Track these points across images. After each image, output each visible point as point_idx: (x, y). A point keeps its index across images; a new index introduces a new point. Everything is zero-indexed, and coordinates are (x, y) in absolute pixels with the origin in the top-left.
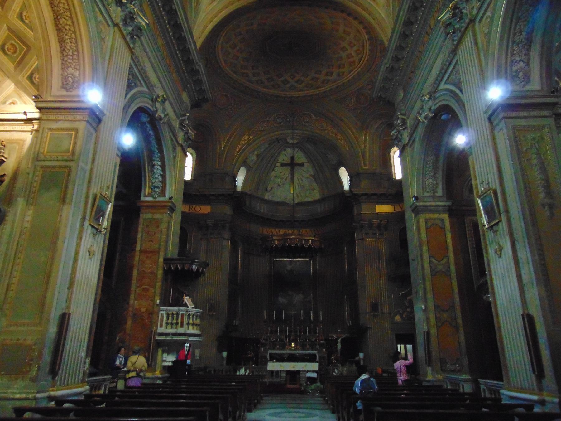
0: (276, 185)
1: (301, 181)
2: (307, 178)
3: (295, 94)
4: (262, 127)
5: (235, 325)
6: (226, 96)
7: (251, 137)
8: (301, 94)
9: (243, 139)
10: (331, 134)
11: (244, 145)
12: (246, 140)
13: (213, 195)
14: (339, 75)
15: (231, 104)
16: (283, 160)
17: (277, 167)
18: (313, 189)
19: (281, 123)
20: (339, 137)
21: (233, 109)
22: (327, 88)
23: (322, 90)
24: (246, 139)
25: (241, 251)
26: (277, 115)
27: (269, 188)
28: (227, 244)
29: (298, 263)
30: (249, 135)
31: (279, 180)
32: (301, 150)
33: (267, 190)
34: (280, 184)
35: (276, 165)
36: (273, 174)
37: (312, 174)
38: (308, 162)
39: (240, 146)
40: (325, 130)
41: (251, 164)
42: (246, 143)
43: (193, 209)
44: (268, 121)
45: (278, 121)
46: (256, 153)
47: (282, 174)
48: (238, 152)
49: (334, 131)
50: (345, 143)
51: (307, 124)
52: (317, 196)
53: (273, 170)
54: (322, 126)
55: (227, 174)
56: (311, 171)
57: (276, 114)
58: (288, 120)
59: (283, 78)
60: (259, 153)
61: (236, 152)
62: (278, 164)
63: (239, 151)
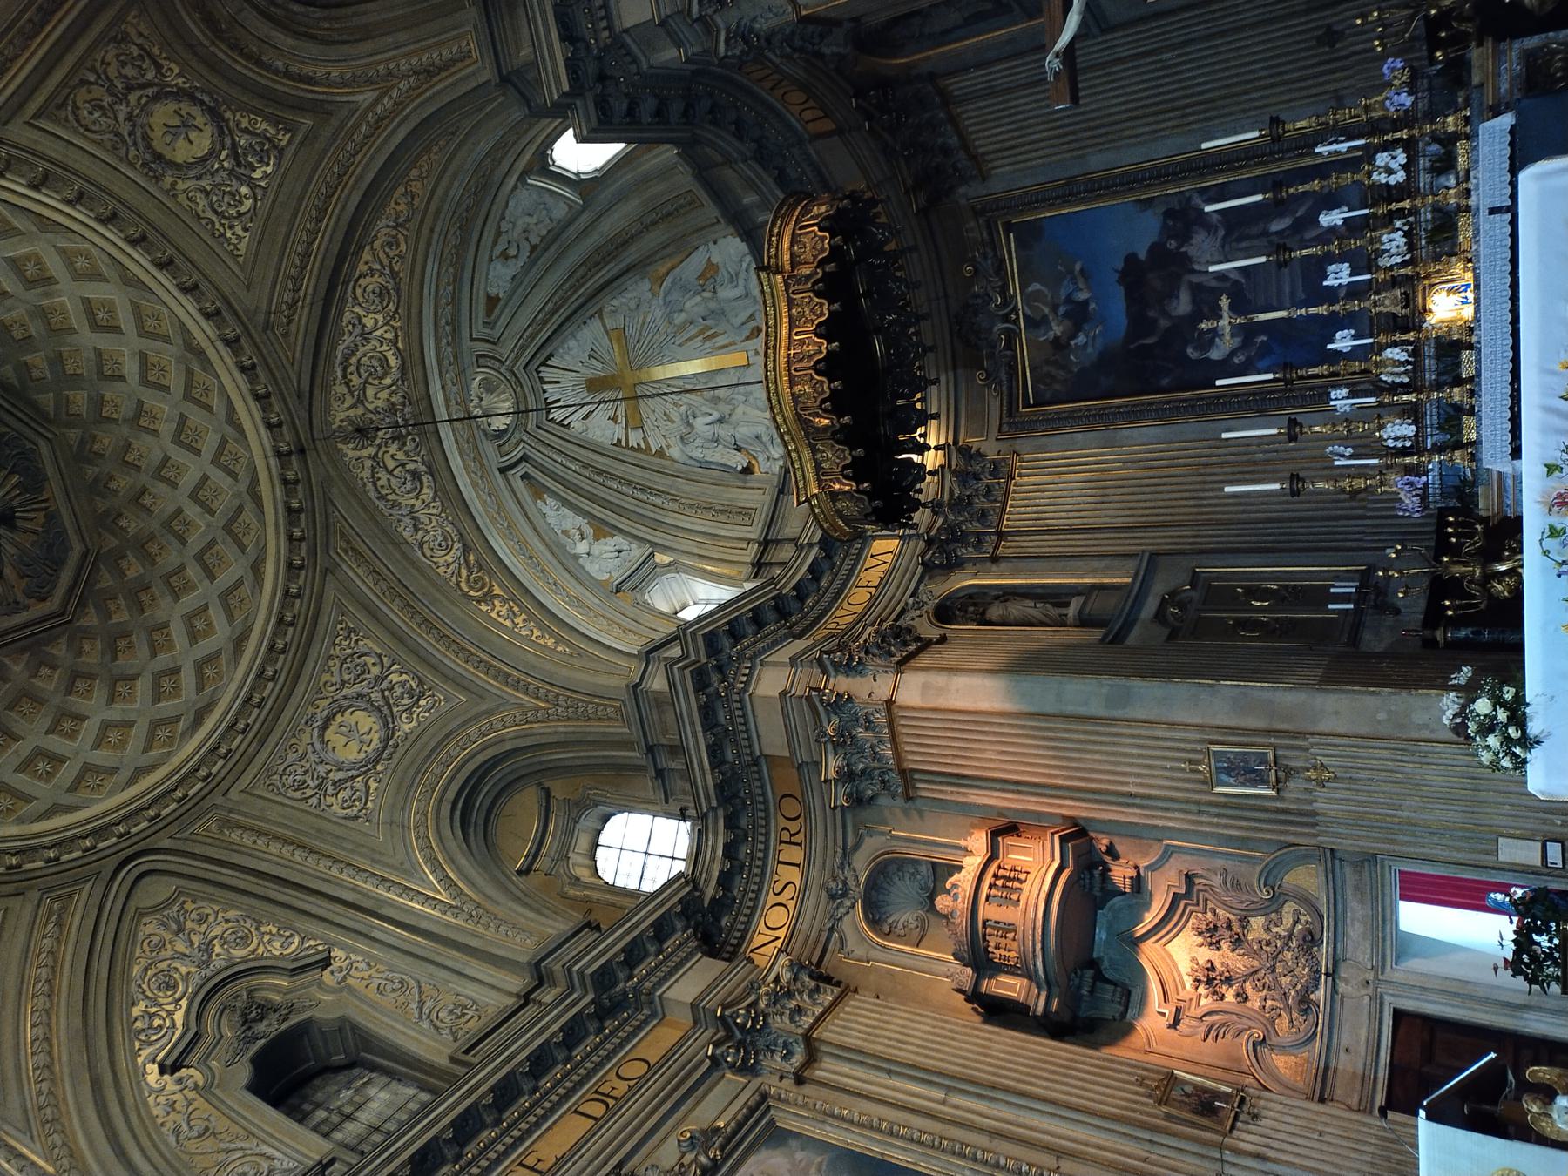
0: (723, 431)
1: (693, 331)
2: (666, 304)
3: (258, 442)
4: (449, 549)
5: (1359, 598)
6: (325, 727)
7: (497, 591)
8: (249, 415)
9: (508, 623)
10: (403, 247)
11: (531, 617)
12: (511, 607)
13: (715, 751)
14: (95, 276)
15: (360, 696)
16: (614, 419)
17: (644, 439)
18: (711, 269)
19: (416, 475)
20: (402, 207)
21: (384, 686)
22: (187, 309)
23: (203, 332)
24: (504, 611)
25: (987, 573)
26: (382, 497)
27: (739, 461)
28: (913, 689)
29: (1036, 286)
30: (489, 597)
31: (699, 423)
32: (551, 356)
33: (747, 470)
34: (716, 416)
35: (638, 449)
36: (675, 452)
37: (645, 285)
38: (600, 313)
39: (537, 633)
40: (394, 275)
41: (637, 552)
42: (523, 609)
43: (794, 826)
44: (416, 529)
45: (409, 486)
46: (582, 548)
47: (674, 415)
48: (559, 640)
49: (383, 228)
50: (414, 173)
51: (393, 361)
52: (730, 249)
53: (661, 454)
54: (382, 293)
55: (636, 686)
56: (639, 289)
57: (381, 504)
58: (395, 446)
59: (192, 511)
60: (588, 531)
61: (559, 649)
62: (635, 438)
63: (552, 634)
